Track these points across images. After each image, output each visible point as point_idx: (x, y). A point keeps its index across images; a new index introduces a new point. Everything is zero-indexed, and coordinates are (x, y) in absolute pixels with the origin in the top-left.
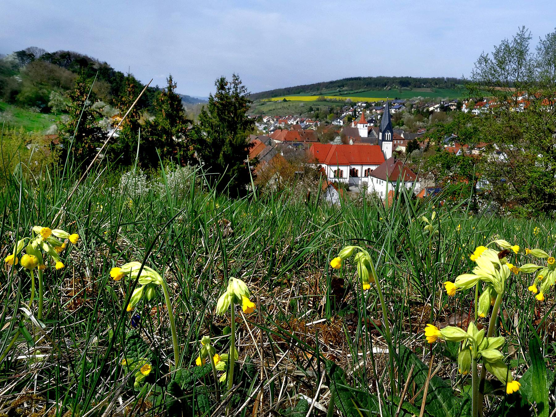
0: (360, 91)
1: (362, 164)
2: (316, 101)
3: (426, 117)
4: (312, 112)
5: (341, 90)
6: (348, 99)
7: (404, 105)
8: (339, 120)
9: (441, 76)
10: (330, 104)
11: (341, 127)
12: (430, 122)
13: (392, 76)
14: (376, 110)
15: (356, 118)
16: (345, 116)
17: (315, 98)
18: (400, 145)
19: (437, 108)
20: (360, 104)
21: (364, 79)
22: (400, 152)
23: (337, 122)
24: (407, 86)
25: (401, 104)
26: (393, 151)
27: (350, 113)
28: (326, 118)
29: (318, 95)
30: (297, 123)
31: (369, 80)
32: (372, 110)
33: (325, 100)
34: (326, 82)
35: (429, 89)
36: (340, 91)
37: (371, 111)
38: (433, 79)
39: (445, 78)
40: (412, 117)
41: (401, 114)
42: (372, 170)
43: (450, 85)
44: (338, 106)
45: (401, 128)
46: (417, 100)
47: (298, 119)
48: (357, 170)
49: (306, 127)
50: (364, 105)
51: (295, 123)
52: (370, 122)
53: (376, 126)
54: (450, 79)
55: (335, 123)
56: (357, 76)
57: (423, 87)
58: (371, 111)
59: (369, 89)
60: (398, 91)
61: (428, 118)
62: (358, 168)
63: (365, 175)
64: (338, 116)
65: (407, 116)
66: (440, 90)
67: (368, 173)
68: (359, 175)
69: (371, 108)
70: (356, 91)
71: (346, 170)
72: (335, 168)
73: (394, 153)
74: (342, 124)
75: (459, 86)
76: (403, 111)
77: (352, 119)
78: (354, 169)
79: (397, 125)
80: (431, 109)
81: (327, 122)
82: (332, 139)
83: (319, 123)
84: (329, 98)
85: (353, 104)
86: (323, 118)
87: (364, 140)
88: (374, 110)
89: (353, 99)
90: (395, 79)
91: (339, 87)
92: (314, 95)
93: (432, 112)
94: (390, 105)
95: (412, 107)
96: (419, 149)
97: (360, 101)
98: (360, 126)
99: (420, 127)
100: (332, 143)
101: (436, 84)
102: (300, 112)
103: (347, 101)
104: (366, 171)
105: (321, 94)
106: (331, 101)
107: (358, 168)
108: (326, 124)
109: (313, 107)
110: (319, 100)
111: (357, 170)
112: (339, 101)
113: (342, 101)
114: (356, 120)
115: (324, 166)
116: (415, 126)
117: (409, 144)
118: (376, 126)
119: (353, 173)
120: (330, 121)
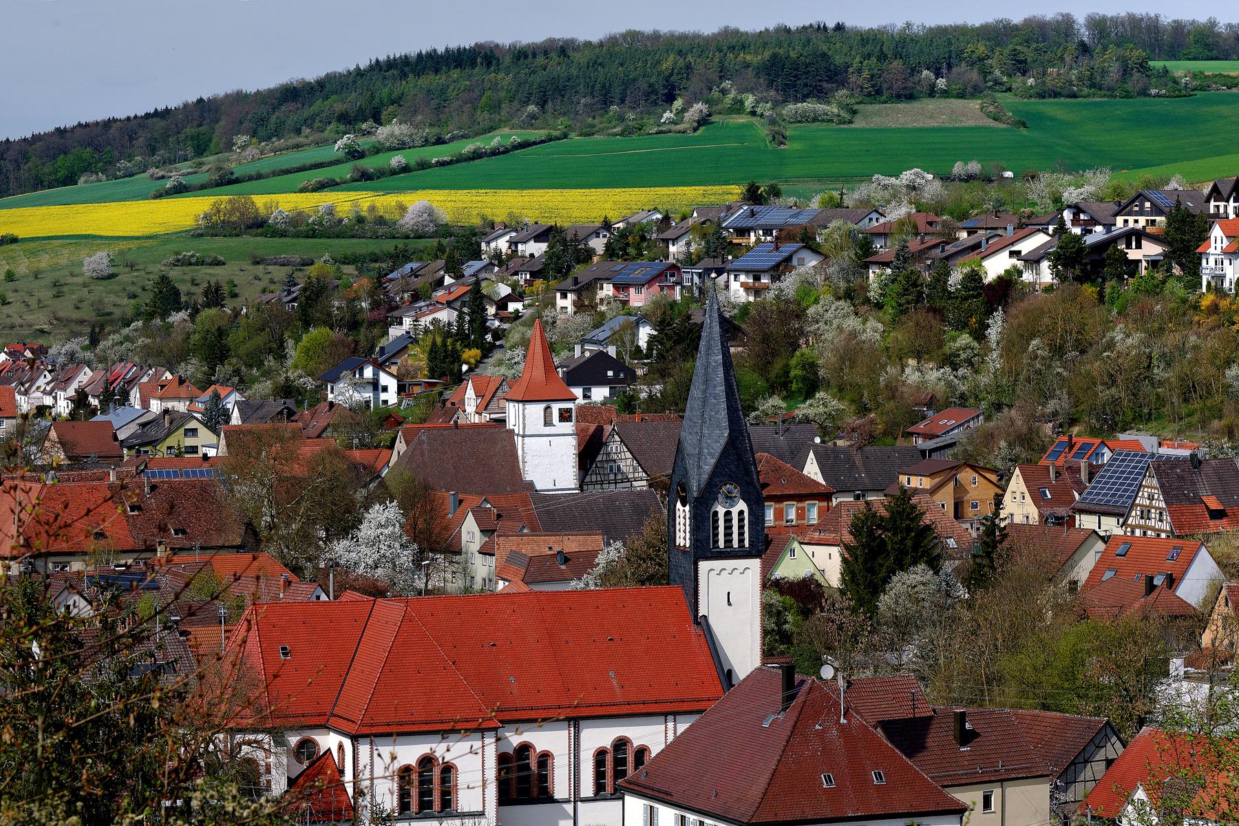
1: (575, 721)
2: (197, 234)
3: (961, 326)
4: (169, 311)
5: (364, 143)
7: (808, 241)
8: (368, 372)
9: (1048, 11)
10: (296, 249)
11: (389, 419)
12: (995, 360)
13: (708, 27)
15: (487, 351)
16: (410, 339)
17: (187, 211)
18: (803, 533)
19: (1033, 261)
20: (502, 244)
21: (522, 55)
22: (806, 593)
23: (357, 386)
24: (820, 94)
25: (785, 235)
26: (764, 586)
27: (445, 315)
28: (281, 357)
29: (203, 188)
30: (80, 400)
31: (556, 68)
33: (258, 225)
34: (250, 87)
35: (975, 104)
36: (354, 154)
37: (585, 291)
38: (997, 34)
39: (1080, 18)
40: (872, 329)
41: (793, 312)
42: (641, 752)
43: (1114, 68)
44: (346, 261)
45: (804, 409)
46: (897, 198)
47: (85, 376)
48: (545, 758)
49: (150, 434)
50: (537, 249)
51: (63, 407)
52: (586, 374)
53: (629, 404)
54: (1115, 21)
55: (343, 393)
56: (467, 42)
57: (932, 92)
58: (585, 291)
60: (764, 131)
61: (980, 335)
62: (549, 740)
63: (599, 787)
64: (358, 345)
65: (834, 326)
66: (1050, 107)
68: (561, 787)
69: (579, 270)
70: (468, 147)
72: (410, 753)
73: (776, 598)
74: (391, 397)
75: (1181, 69)
76: (807, 286)
77: (457, 359)
78: (525, 748)
79: (772, 390)
80: (996, 267)
81: (287, 390)
82: (345, 523)
83: (232, 401)
84: (284, 203)
85: (461, 244)
86: (255, 360)
87: (552, 513)
88: (608, 290)
90: (731, 44)
91: (348, 120)
92: (180, 190)
93: (1006, 286)
94: (719, 249)
95: (865, 255)
96: (934, 564)
97: (500, 217)
98: (524, 418)
99: (932, 402)
100: (341, 549)
101: (1020, 66)
102: (87, 314)
103: (408, 221)
104: (600, 755)
105: (226, 181)
107: (549, 740)
108: (278, 405)
109: (175, 274)
110: (213, 228)
111: (545, 758)
112: (359, 225)
113: (379, 226)
114: (491, 370)
115: (329, 741)
116: (893, 391)
117: (865, 527)
118: (629, 404)
120: (310, 383)
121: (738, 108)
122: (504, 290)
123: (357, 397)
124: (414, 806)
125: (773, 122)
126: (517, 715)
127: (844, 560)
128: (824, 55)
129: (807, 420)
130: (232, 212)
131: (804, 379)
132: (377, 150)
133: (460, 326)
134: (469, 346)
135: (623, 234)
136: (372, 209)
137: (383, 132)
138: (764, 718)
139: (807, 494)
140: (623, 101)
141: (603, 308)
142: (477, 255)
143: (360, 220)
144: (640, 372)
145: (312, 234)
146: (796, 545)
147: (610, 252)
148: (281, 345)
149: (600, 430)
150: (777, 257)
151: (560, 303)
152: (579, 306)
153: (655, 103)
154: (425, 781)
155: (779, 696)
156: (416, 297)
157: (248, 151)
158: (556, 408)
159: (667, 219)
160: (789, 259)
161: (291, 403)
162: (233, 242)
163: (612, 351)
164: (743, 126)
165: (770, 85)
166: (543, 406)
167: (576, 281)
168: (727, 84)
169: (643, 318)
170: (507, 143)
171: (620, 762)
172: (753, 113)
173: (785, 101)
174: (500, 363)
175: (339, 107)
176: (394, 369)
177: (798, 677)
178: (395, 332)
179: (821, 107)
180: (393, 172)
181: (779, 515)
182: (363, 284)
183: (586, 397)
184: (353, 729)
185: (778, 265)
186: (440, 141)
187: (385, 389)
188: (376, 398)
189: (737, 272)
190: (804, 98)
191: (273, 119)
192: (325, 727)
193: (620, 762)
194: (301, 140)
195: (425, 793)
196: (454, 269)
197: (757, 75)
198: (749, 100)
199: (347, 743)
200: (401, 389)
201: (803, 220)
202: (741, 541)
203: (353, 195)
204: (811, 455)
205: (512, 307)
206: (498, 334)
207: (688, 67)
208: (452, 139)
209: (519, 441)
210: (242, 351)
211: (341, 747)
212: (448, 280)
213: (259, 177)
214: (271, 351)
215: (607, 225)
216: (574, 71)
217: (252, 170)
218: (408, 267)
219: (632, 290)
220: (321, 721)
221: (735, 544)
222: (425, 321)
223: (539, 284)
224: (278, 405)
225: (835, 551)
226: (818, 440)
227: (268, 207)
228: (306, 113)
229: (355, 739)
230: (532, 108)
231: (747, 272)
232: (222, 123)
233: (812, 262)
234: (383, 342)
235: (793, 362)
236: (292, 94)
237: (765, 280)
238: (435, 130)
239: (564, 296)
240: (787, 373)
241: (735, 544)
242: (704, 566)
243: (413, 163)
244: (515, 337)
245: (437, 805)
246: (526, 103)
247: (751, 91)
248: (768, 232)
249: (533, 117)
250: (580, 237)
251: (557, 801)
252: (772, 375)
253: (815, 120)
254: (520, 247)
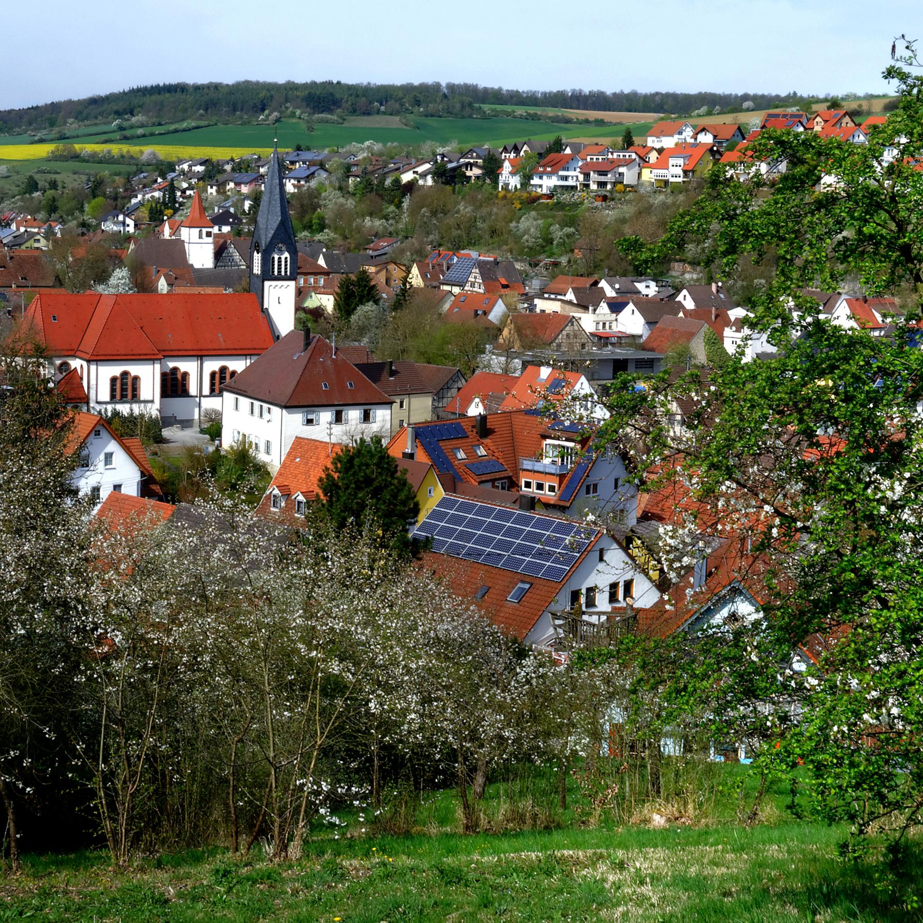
0: (185, 125)
1: (200, 356)
2: (48, 160)
3: (391, 202)
5: (125, 124)
6: (147, 151)
7: (322, 166)
8: (121, 218)
9: (430, 80)
10: (93, 168)
11: (128, 238)
12: (405, 218)
13: (281, 80)
14: (238, 184)
15: (176, 211)
16: (141, 204)
17: (43, 150)
18: (317, 290)
19: (424, 175)
20: (185, 167)
21: (197, 88)
22: (317, 313)
23: (115, 223)
24: (330, 111)
25: (312, 163)
27: (157, 194)
28: (81, 210)
29: (51, 141)
32: (225, 183)
33: (76, 157)
34: (75, 98)
35: (397, 118)
36: (121, 128)
37: (221, 186)
38: (408, 89)
39: (444, 84)
40: (350, 203)
41: (314, 195)
42: (233, 373)
43: (458, 106)
44: (116, 174)
45: (318, 237)
46: (362, 151)
48: (185, 375)
49: (18, 241)
50: (199, 169)
52: (220, 220)
53: (239, 233)
54: (459, 86)
55: (109, 226)
57: (378, 112)
58: (221, 186)
59: (214, 119)
60: (303, 126)
61: (399, 206)
62: (188, 366)
63: (212, 390)
65: (332, 202)
66: (430, 121)
67: (221, 383)
68: (193, 390)
69: (220, 178)
70: (172, 127)
71: (148, 376)
72: (116, 370)
73: (302, 315)
74: (131, 229)
75: (486, 107)
76: (321, 184)
77: (161, 213)
78: (175, 369)
79: (305, 228)
80: (407, 177)
81: (84, 225)
82: (103, 277)
83: (57, 228)
84: (88, 148)
86: (70, 213)
87: (201, 277)
88: (232, 185)
89: (163, 151)
90: (291, 87)
91: (118, 114)
92: (41, 141)
93: (411, 185)
95: (347, 171)
96: (376, 302)
97: (186, 156)
98: (188, 234)
99: (376, 235)
100: (100, 288)
101: (418, 103)
104: (213, 375)
105: (62, 138)
106: (94, 159)
107: (188, 366)
108: (80, 230)
109: (37, 177)
110: (54, 158)
111: (185, 375)
112: (123, 159)
114: (177, 218)
115: (75, 363)
116: (359, 230)
118: (239, 233)
119: (174, 386)
120: (94, 222)
121: (293, 115)
122: (185, 185)
123: (115, 228)
124: (118, 397)
125: (308, 122)
126: (171, 353)
127: (335, 299)
128: (332, 94)
129: (319, 241)
130: (64, 151)
131: (319, 224)
132: (132, 127)
133: (164, 199)
134: (168, 208)
135: (239, 163)
136: (128, 152)
137: (134, 119)
138: (293, 354)
139: (319, 272)
140: (242, 110)
141: (229, 193)
142: (174, 171)
143: (123, 157)
144: (244, 221)
145: (100, 162)
146: (313, 294)
147: (233, 170)
148: (82, 206)
149: (226, 242)
150: (308, 172)
151: (210, 190)
152: (218, 192)
153: (256, 112)
154: (123, 384)
155: (302, 344)
156: (144, 187)
157: (73, 126)
158: (204, 230)
159: (259, 157)
160: (313, 173)
161: (84, 230)
162: (65, 164)
163: (232, 210)
164: (295, 123)
165: (308, 105)
166: (198, 229)
167: (217, 181)
168: (288, 105)
169: (247, 197)
170: (190, 126)
171: (222, 378)
172: (300, 118)
173: (314, 113)
174: (181, 215)
175: (115, 108)
176: (133, 217)
177: (312, 335)
178: (134, 201)
179: (329, 116)
180: (138, 137)
181: (306, 281)
182: (119, 180)
183: (220, 230)
184: (88, 357)
185: (308, 177)
186: (160, 124)
187: (128, 225)
188: (124, 229)
189: (290, 178)
190: (322, 112)
191: (85, 112)
192: (74, 356)
193: (222, 378)
194: (98, 121)
195: (123, 390)
196: (163, 175)
197: (302, 101)
198: (298, 112)
199: (85, 364)
200: (136, 225)
201: (320, 158)
202: (286, 272)
203: (120, 146)
204: (321, 256)
205: (188, 192)
206: (181, 204)
207: (272, 96)
208: (166, 124)
209: (186, 245)
210: (64, 208)
211: (82, 366)
212: (159, 180)
213: (78, 137)
214: (77, 209)
215: (232, 160)
216: (221, 96)
217: (75, 133)
218: (142, 175)
219: (243, 186)
220: (72, 353)
221: (283, 273)
222: (148, 196)
223: (201, 182)
224: (80, 230)
225: (331, 298)
226: (324, 250)
227: (81, 149)
228: (100, 110)
229: (89, 361)
230: (201, 111)
231: (295, 178)
232: (62, 113)
233: (324, 175)
234: (128, 205)
235: (314, 216)
236: (95, 101)
237: (302, 183)
238: (158, 120)
239: (212, 188)
240: (311, 221)
241: (283, 273)
242: (267, 284)
243: (147, 133)
244: (188, 204)
245: (130, 396)
246: (199, 109)
247: (299, 108)
248: (304, 163)
249: (202, 115)
250: (220, 163)
251: (192, 396)
252: (305, 222)
253: (327, 122)
254: (193, 168)
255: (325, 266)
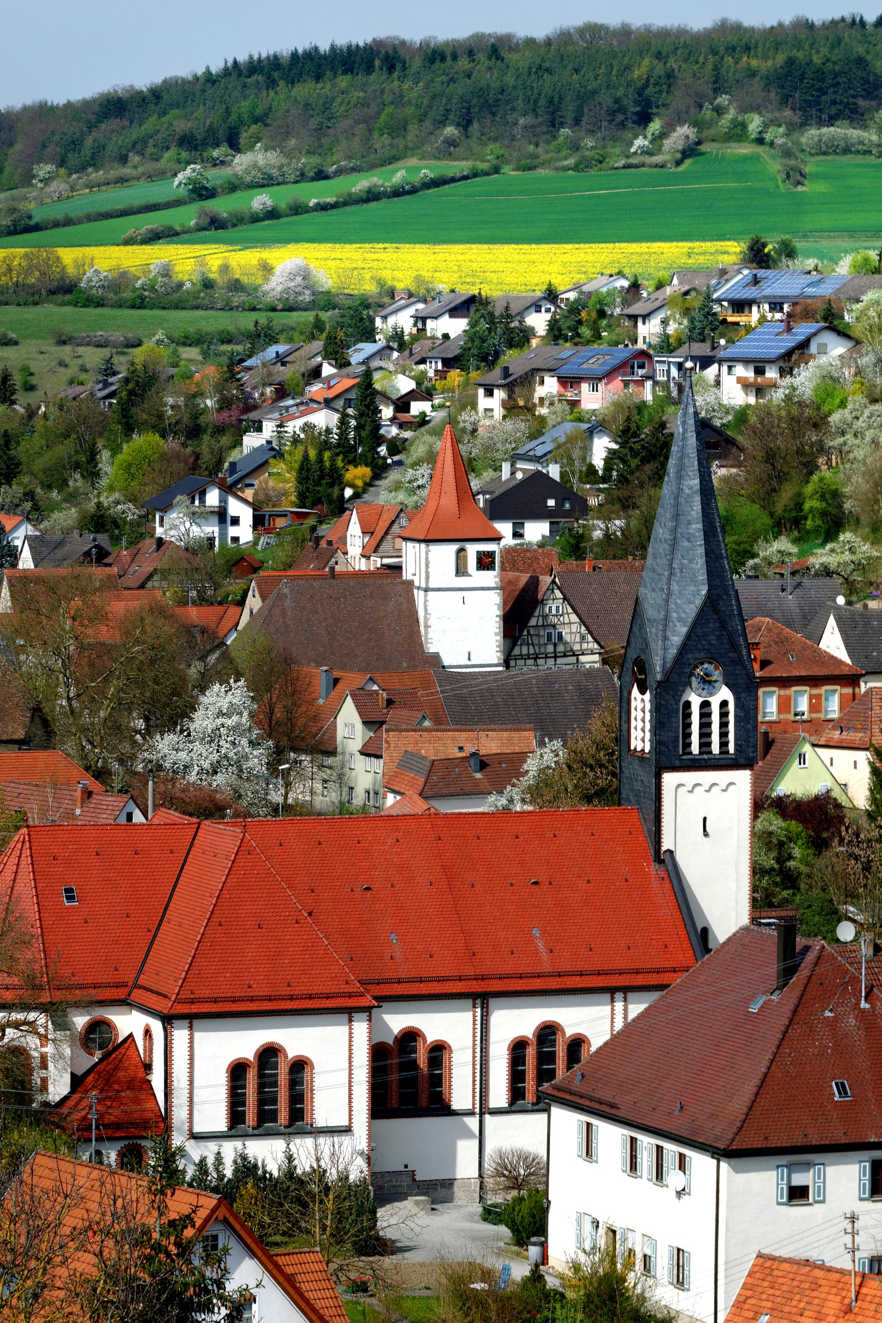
0: (398, 176)
1: (482, 998)
5: (215, 177)
6: (286, 264)
7: (831, 320)
8: (213, 497)
10: (120, 323)
11: (241, 563)
14: (569, 381)
15: (379, 470)
16: (273, 452)
18: (818, 731)
20: (404, 321)
21: (437, 55)
23: (195, 517)
24: (855, 115)
25: (800, 310)
27: (324, 419)
28: (92, 474)
31: (486, 75)
32: (529, 378)
33: (65, 290)
34: (58, 97)
36: (201, 192)
37: (518, 385)
42: (577, 1044)
44: (187, 341)
45: (823, 556)
48: (439, 1050)
50: (455, 327)
52: (516, 504)
53: (576, 547)
55: (177, 526)
56: (361, 37)
58: (518, 385)
59: (492, 151)
60: (774, 166)
62: (446, 1026)
63: (516, 1093)
64: (200, 458)
67: (544, 1074)
68: (461, 1093)
69: (511, 358)
70: (360, 184)
71: (335, 1057)
72: (244, 1042)
73: (775, 823)
74: (244, 532)
77: (336, 479)
78: (411, 1036)
79: (779, 527)
81: (99, 521)
82: (172, 712)
85: (348, 321)
87: (465, 699)
88: (550, 386)
89: (334, 264)
91: (192, 144)
94: (708, 329)
97: (403, 282)
98: (428, 565)
100: (165, 746)
103: (275, 286)
104: (518, 1047)
106: (124, 295)
107: (446, 1026)
108: (86, 541)
111: (439, 1050)
113: (235, 292)
114: (384, 496)
115: (129, 1023)
118: (576, 547)
119: (406, 1083)
120: (131, 512)
121: (738, 133)
122: (405, 385)
123: (196, 532)
124: (251, 1117)
125: (787, 153)
126: (399, 989)
127: (875, 771)
128: (860, 62)
129: (827, 572)
130: (28, 271)
131: (824, 514)
132: (233, 187)
133: (343, 434)
134: (354, 462)
135: (575, 309)
136: (225, 268)
137: (241, 162)
138: (751, 999)
139: (828, 676)
140: (577, 121)
141: (543, 411)
142: (369, 335)
143: (208, 284)
144: (593, 502)
145: (139, 303)
146: (807, 748)
147: (555, 333)
148: (93, 458)
149: (534, 583)
150: (788, 342)
151: (483, 402)
152: (510, 408)
153: (622, 125)
154: (266, 1082)
155: (773, 968)
156: (282, 392)
157: (54, 186)
158: (472, 550)
159: (635, 287)
160: (804, 345)
161: (103, 539)
162: (29, 313)
163: (554, 471)
164: (745, 159)
165: (785, 100)
166: (453, 548)
167: (506, 372)
168: (723, 99)
169: (599, 426)
170: (416, 179)
171: (546, 1058)
172: (760, 141)
173: (804, 125)
174: (397, 487)
175: (182, 126)
176: (249, 494)
177: (800, 941)
178: (252, 441)
179: (854, 134)
180: (255, 219)
181: (784, 705)
182: (208, 373)
183: (517, 535)
184: (165, 1006)
185: (788, 354)
186: (321, 175)
187: (235, 521)
188: (223, 534)
189: (732, 362)
190: (831, 121)
191: (89, 141)
192: (125, 1003)
193: (546, 1058)
194: (127, 171)
195: (266, 1100)
196: (337, 354)
197: (766, 88)
198: (755, 123)
199: (157, 1026)
200: (258, 521)
201: (826, 290)
202: (724, 744)
203: (199, 250)
204: (832, 622)
205: (417, 408)
206: (396, 447)
207: (670, 75)
208: (339, 172)
209: (419, 596)
210: (38, 465)
211: (148, 1032)
212: (328, 370)
213: (68, 222)
214: (77, 466)
215: (551, 295)
216: (510, 80)
217: (58, 212)
218: (271, 352)
219: (585, 387)
220: (121, 993)
221: (715, 749)
222: (294, 426)
223: (455, 376)
224: (86, 541)
225: (863, 758)
226: (841, 600)
227: (79, 265)
228: (135, 133)
229: (168, 1020)
230: (450, 130)
231: (746, 361)
232: (18, 147)
233: (837, 349)
234: (234, 456)
235: (809, 489)
236: (116, 107)
237: (772, 374)
238: (315, 160)
239: (489, 393)
240: (799, 506)
241: (715, 749)
242: (669, 779)
243: (283, 206)
244: (419, 450)
245: (283, 1116)
246: (442, 123)
247: (758, 109)
248: (776, 306)
249: (452, 143)
250: (514, 311)
251: (454, 1113)
252: (779, 509)
253: (847, 151)
254: (430, 324)
255: (848, 661)
